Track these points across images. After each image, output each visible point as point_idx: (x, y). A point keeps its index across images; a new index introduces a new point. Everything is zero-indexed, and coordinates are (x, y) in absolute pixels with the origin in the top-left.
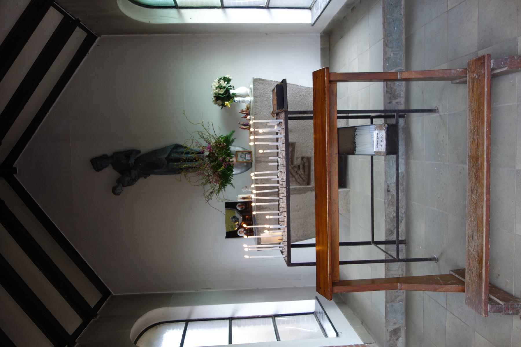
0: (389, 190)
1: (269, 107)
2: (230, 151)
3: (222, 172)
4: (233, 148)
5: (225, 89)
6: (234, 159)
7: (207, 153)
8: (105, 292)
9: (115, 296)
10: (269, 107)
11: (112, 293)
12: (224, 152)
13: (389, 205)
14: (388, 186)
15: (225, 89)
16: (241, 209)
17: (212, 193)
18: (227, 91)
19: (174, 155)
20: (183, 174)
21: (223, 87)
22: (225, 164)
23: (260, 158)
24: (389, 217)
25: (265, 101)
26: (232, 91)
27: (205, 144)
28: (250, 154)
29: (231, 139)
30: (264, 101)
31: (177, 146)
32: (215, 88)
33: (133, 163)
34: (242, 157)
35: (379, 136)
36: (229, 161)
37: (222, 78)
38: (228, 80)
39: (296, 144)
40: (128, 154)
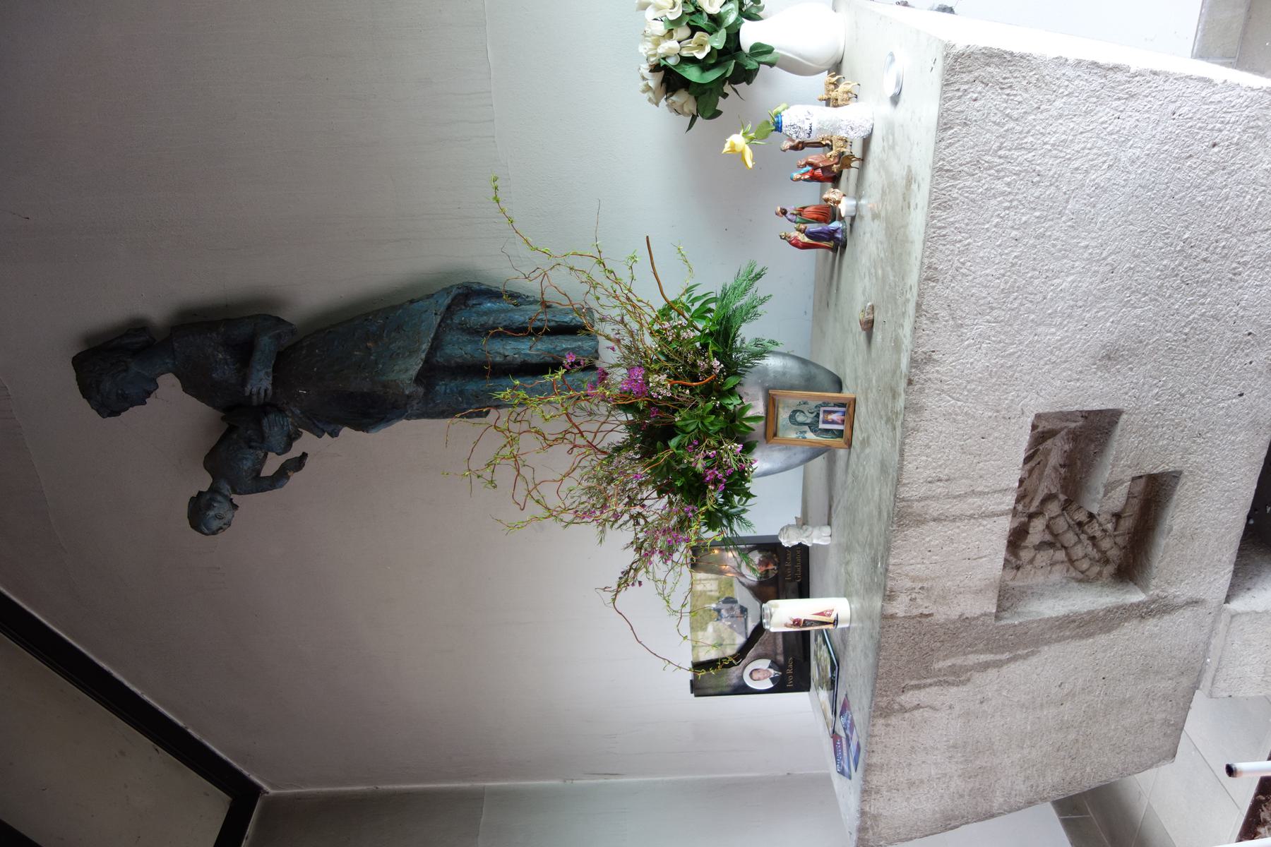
1: (1014, 233)
10: (1014, 233)
11: (265, 787)
19: (459, 349)
21: (710, 16)
23: (922, 504)
25: (1003, 193)
30: (994, 196)
32: (660, 28)
33: (266, 391)
34: (800, 418)
39: (1124, 417)
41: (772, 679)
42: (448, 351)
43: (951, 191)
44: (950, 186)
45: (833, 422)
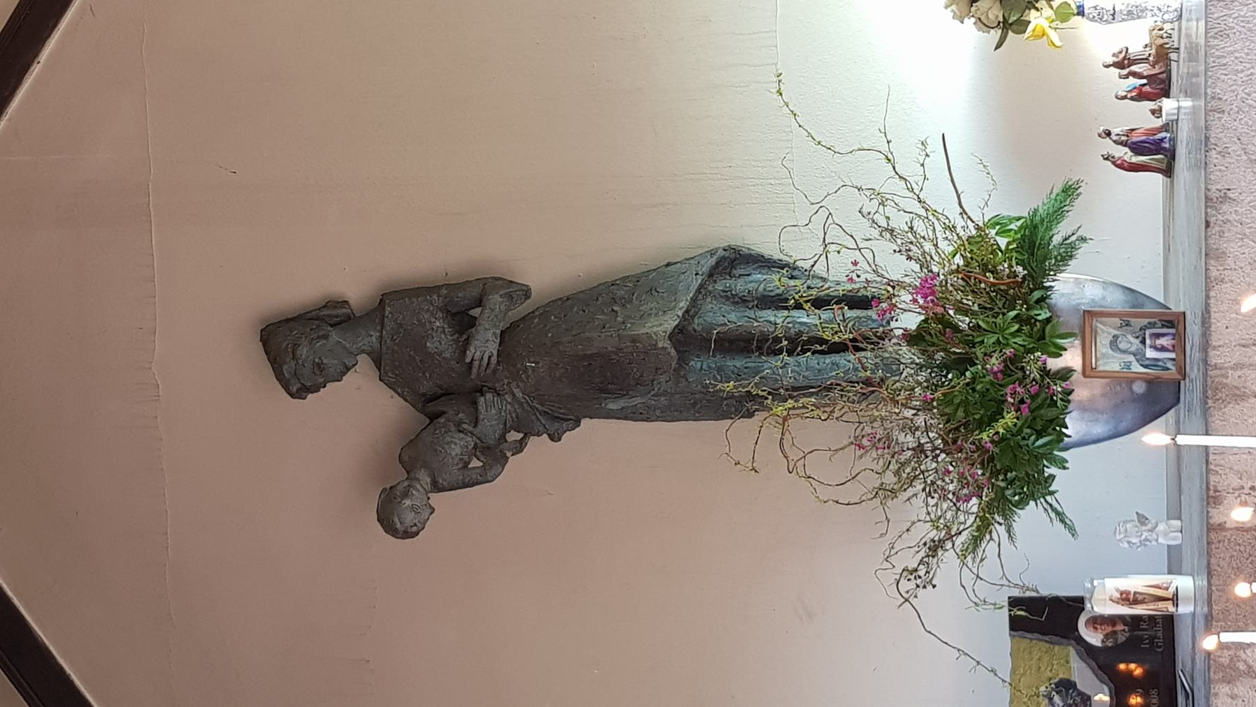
2: (1050, 308)
6: (1071, 358)
7: (910, 321)
27: (899, 268)
29: (1057, 239)
36: (1045, 372)
42: (709, 320)
43: (1225, 20)
44: (1225, 15)
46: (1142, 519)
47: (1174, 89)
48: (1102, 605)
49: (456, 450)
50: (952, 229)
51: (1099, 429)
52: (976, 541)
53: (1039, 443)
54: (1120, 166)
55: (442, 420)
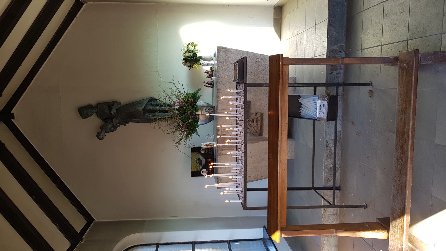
0: (328, 146)
2: (196, 105)
3: (189, 123)
4: (199, 103)
5: (193, 53)
6: (199, 113)
7: (177, 107)
8: (89, 219)
9: (97, 222)
11: (95, 219)
12: (192, 107)
13: (327, 158)
14: (327, 143)
15: (193, 53)
16: (205, 153)
17: (181, 139)
18: (195, 54)
19: (150, 107)
20: (157, 123)
21: (192, 51)
22: (192, 116)
24: (327, 168)
26: (198, 55)
27: (175, 100)
28: (213, 109)
31: (152, 99)
32: (184, 52)
33: (114, 113)
34: (206, 111)
35: (322, 105)
36: (196, 114)
37: (190, 43)
38: (195, 46)
39: (251, 102)
40: (110, 105)
41: (206, 173)
45: (212, 111)
46: (209, 135)
47: (214, 76)
48: (204, 147)
49: (109, 127)
50: (183, 94)
51: (203, 123)
52: (186, 138)
53: (195, 124)
54: (206, 87)
55: (107, 122)
